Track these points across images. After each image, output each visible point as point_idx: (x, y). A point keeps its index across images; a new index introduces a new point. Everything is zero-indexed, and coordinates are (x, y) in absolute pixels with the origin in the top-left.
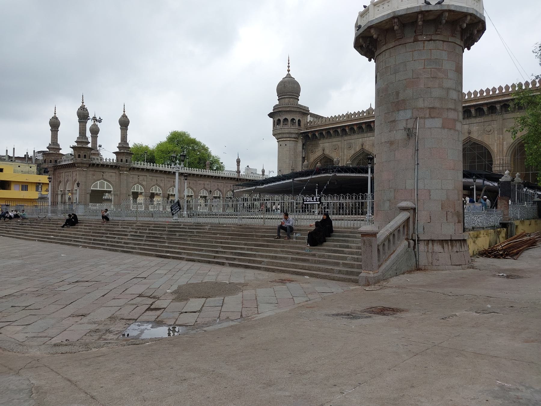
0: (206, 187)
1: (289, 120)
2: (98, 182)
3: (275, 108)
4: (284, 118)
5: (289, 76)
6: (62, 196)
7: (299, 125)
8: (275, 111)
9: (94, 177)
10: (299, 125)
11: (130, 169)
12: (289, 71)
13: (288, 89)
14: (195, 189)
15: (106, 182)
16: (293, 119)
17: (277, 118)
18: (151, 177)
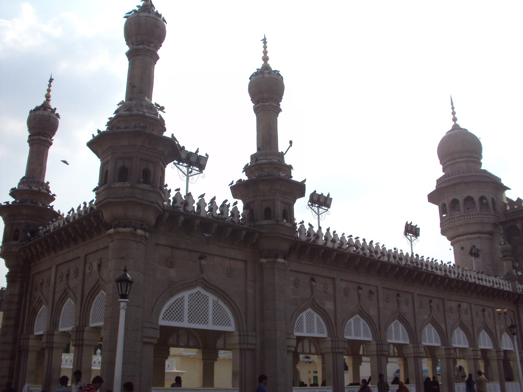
0: (466, 318)
1: (476, 199)
2: (186, 295)
3: (440, 181)
4: (465, 195)
5: (456, 127)
6: (40, 354)
7: (495, 209)
8: (439, 187)
9: (173, 273)
10: (495, 209)
11: (292, 249)
12: (455, 120)
13: (460, 151)
14: (443, 327)
15: (212, 298)
16: (482, 198)
17: (451, 199)
18: (343, 285)
